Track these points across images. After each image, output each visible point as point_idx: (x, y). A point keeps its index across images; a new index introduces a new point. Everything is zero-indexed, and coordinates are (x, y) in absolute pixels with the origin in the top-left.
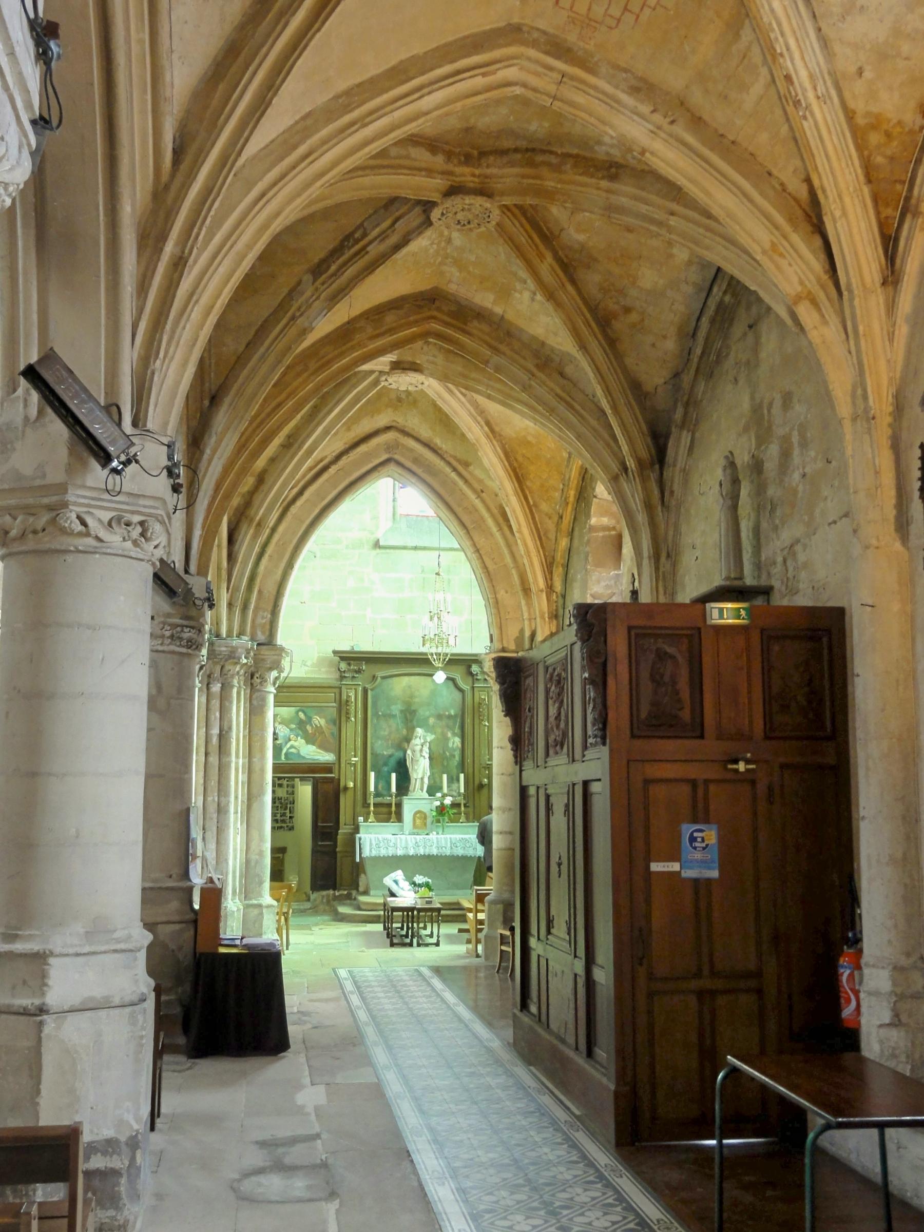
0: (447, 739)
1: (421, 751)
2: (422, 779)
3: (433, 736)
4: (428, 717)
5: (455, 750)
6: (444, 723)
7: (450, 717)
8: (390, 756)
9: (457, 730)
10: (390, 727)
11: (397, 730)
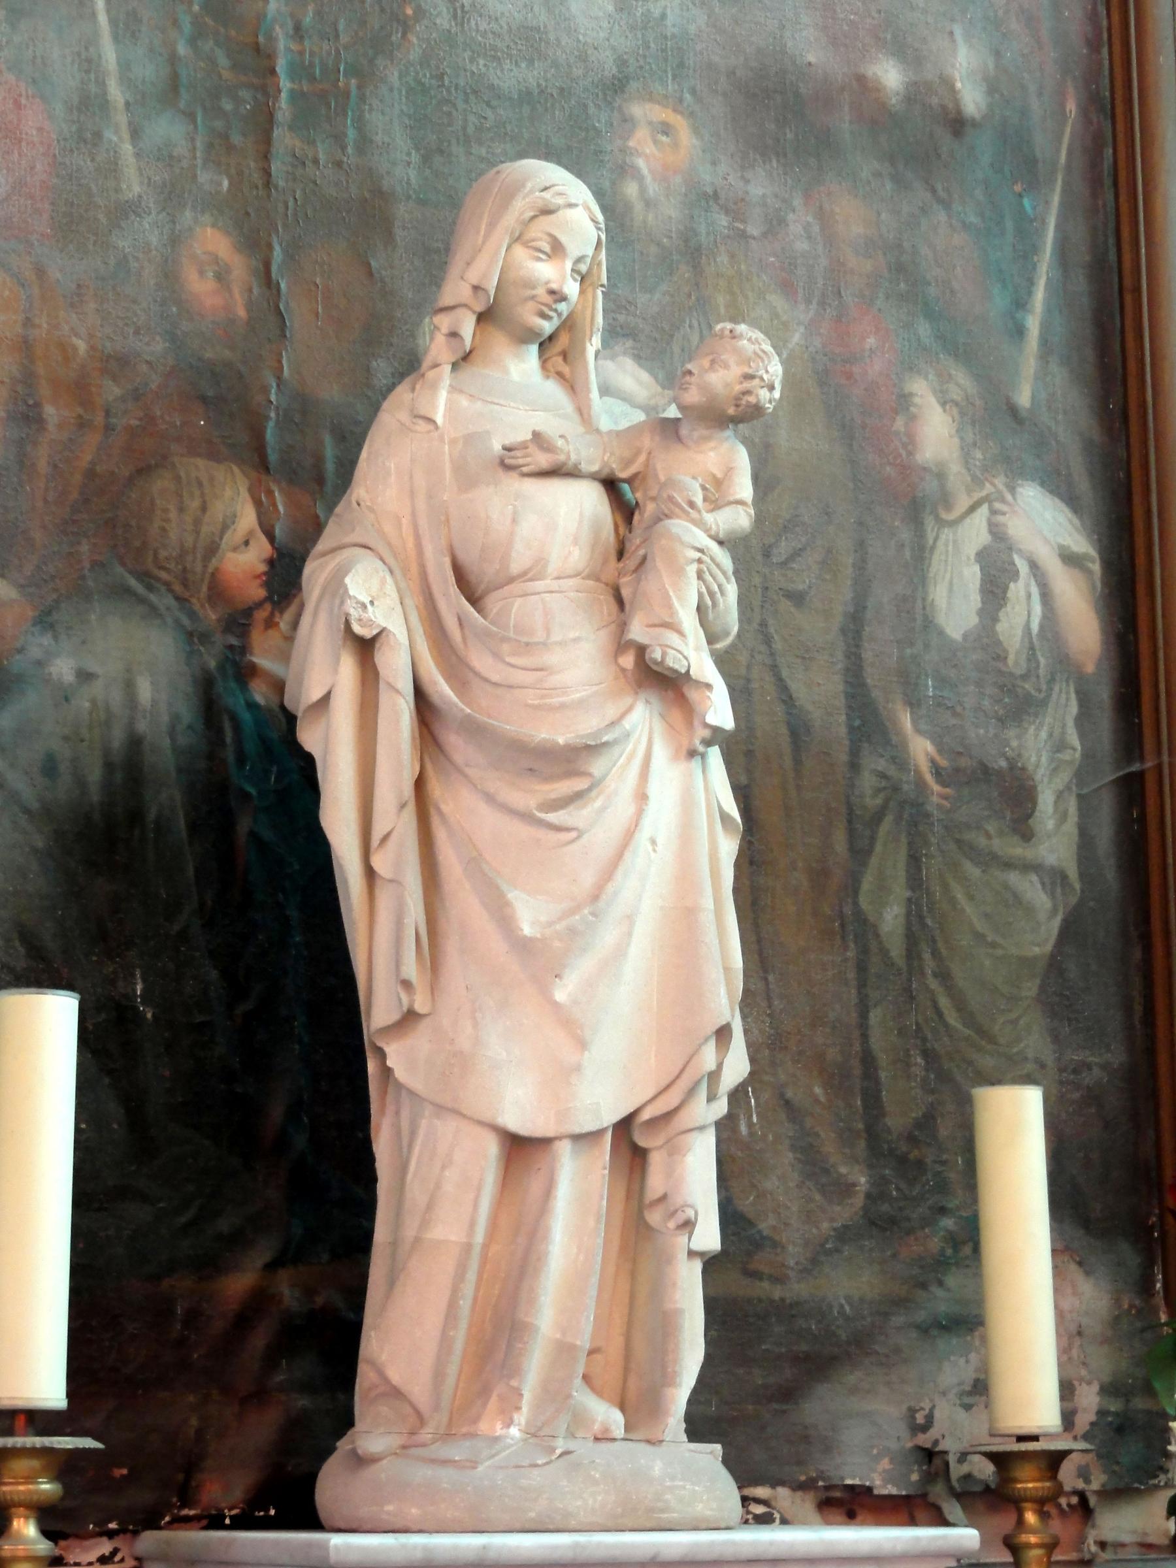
0: (912, 505)
4: (616, 87)
5: (1020, 706)
6: (853, 213)
7: (924, 140)
9: (1040, 373)
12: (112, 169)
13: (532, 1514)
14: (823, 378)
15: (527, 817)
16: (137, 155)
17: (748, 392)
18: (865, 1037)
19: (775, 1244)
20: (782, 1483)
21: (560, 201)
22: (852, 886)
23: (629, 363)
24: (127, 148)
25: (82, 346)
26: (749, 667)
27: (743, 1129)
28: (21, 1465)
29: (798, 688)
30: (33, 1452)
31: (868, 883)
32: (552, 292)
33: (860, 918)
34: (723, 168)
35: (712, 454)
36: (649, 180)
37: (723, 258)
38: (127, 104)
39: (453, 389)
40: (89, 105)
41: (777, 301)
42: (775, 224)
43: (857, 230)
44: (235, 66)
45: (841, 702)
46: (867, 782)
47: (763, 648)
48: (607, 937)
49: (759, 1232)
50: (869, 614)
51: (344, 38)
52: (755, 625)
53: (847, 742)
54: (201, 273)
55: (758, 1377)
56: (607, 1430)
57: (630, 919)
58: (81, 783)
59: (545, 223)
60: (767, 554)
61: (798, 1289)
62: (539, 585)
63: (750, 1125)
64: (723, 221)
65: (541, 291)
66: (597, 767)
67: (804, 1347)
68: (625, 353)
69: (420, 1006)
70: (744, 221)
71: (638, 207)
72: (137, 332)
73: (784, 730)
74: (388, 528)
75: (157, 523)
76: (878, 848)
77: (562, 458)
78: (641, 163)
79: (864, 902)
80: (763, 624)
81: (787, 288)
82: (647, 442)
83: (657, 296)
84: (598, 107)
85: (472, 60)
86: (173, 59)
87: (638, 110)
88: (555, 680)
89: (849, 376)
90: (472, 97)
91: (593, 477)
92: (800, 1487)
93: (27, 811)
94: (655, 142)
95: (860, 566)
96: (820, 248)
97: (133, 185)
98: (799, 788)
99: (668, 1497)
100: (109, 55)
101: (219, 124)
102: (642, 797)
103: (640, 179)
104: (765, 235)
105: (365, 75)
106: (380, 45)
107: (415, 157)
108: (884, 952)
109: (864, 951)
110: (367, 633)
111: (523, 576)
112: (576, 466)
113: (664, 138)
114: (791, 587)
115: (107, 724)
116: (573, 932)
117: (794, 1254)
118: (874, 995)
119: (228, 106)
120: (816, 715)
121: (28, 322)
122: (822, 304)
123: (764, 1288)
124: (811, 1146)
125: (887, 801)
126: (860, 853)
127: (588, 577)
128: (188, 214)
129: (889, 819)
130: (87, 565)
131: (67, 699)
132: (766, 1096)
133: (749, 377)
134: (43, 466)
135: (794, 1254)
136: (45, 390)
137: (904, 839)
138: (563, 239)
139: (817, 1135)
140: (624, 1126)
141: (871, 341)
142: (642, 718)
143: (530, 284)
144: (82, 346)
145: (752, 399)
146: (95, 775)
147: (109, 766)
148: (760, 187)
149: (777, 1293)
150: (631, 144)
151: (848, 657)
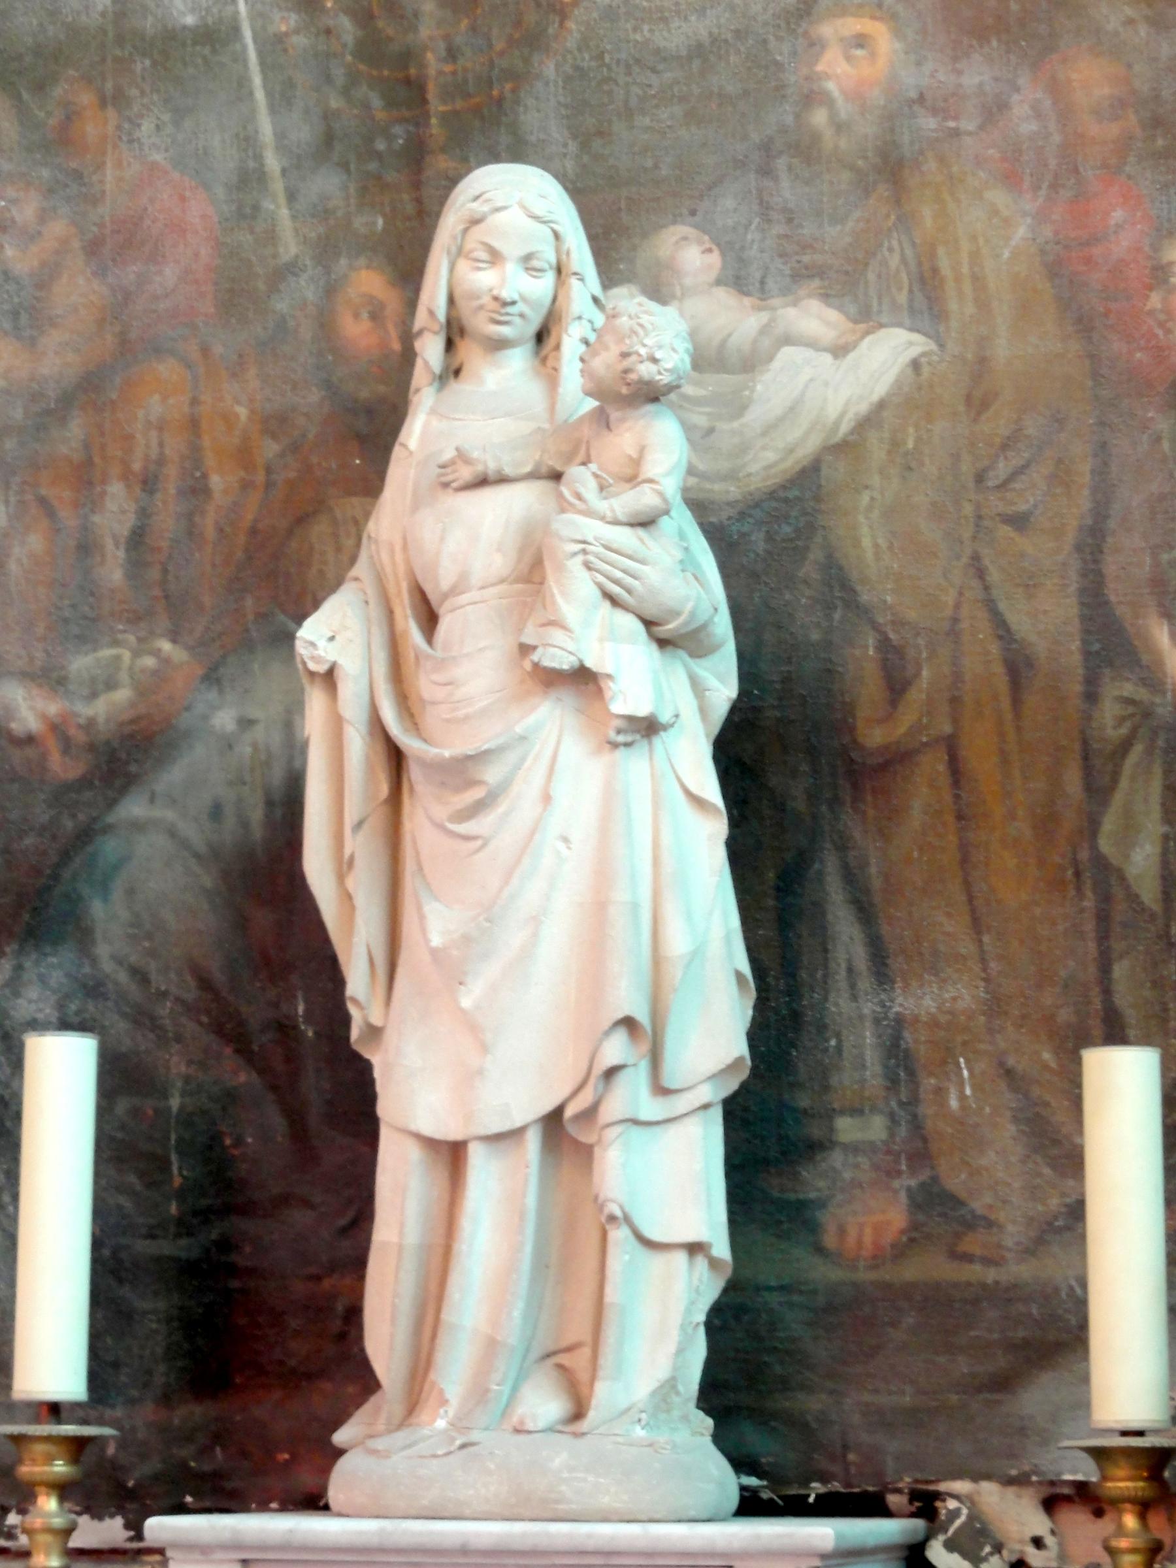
1: (532, 571)
2: (563, 1135)
3: (887, 356)
8: (124, 758)
10: (116, 244)
11: (239, 290)
12: (271, 237)
13: (425, 1502)
14: (1054, 270)
15: (441, 827)
16: (294, 218)
17: (626, 371)
18: (1107, 992)
19: (990, 1224)
20: (988, 1477)
21: (485, 208)
22: (1092, 826)
23: (815, 305)
24: (284, 212)
25: (242, 412)
26: (957, 606)
27: (954, 1103)
28: (39, 1448)
29: (1020, 621)
30: (48, 1439)
31: (1109, 824)
32: (496, 299)
33: (1101, 863)
34: (928, 67)
35: (627, 435)
36: (840, 102)
37: (931, 165)
38: (284, 171)
39: (433, 411)
40: (250, 179)
41: (999, 197)
42: (994, 110)
43: (1103, 91)
44: (390, 103)
45: (1075, 627)
46: (1108, 712)
47: (975, 583)
48: (513, 939)
49: (972, 1212)
50: (1112, 524)
51: (499, 45)
52: (965, 560)
53: (1080, 671)
54: (356, 316)
55: (963, 1366)
56: (522, 1422)
57: (536, 921)
58: (245, 824)
59: (477, 233)
60: (980, 478)
61: (1019, 1271)
62: (464, 598)
63: (962, 1097)
64: (929, 123)
65: (486, 300)
66: (492, 774)
67: (1021, 1333)
68: (809, 296)
69: (376, 1019)
70: (956, 118)
71: (828, 134)
72: (294, 387)
73: (999, 669)
74: (385, 557)
75: (314, 570)
76: (1124, 783)
77: (480, 468)
78: (831, 86)
79: (1105, 845)
80: (976, 557)
81: (1011, 179)
82: (586, 431)
83: (850, 224)
84: (779, 39)
85: (635, 29)
86: (328, 116)
87: (827, 30)
88: (460, 693)
89: (1088, 261)
90: (636, 69)
91: (533, 476)
92: (1010, 1482)
93: (197, 856)
94: (849, 58)
95: (1101, 472)
96: (1052, 126)
97: (290, 247)
98: (1019, 729)
99: (563, 1488)
100: (266, 128)
101: (373, 166)
102: (547, 799)
103: (826, 100)
104: (981, 127)
105: (519, 78)
106: (533, 41)
107: (573, 147)
108: (1133, 898)
109: (1106, 898)
110: (322, 668)
111: (455, 591)
112: (499, 472)
113: (859, 52)
114: (1010, 510)
115: (267, 764)
116: (467, 939)
117: (1013, 1233)
118: (1118, 946)
119: (381, 145)
120: (1040, 648)
121: (194, 402)
122: (1054, 187)
123: (975, 1272)
124: (1037, 1114)
125: (1134, 731)
126: (1098, 791)
127: (518, 580)
128: (343, 261)
129: (1138, 749)
130: (251, 617)
131: (230, 747)
132: (981, 1066)
133: (625, 355)
134: (210, 533)
135: (1013, 1233)
136: (210, 460)
137: (1158, 770)
138: (496, 244)
139: (1047, 1104)
140: (553, 1121)
141: (1118, 215)
142: (551, 719)
143: (474, 296)
144: (242, 412)
145: (633, 377)
146: (257, 815)
147: (270, 803)
148: (977, 75)
149: (991, 1275)
150: (820, 68)
151: (1084, 575)
